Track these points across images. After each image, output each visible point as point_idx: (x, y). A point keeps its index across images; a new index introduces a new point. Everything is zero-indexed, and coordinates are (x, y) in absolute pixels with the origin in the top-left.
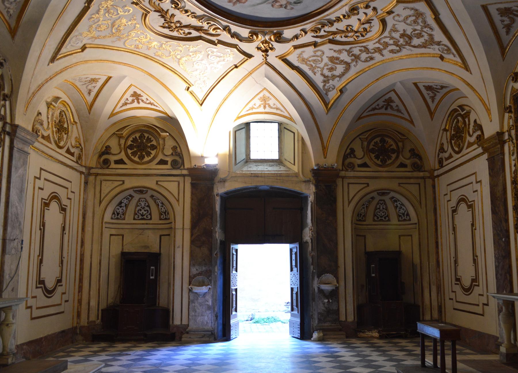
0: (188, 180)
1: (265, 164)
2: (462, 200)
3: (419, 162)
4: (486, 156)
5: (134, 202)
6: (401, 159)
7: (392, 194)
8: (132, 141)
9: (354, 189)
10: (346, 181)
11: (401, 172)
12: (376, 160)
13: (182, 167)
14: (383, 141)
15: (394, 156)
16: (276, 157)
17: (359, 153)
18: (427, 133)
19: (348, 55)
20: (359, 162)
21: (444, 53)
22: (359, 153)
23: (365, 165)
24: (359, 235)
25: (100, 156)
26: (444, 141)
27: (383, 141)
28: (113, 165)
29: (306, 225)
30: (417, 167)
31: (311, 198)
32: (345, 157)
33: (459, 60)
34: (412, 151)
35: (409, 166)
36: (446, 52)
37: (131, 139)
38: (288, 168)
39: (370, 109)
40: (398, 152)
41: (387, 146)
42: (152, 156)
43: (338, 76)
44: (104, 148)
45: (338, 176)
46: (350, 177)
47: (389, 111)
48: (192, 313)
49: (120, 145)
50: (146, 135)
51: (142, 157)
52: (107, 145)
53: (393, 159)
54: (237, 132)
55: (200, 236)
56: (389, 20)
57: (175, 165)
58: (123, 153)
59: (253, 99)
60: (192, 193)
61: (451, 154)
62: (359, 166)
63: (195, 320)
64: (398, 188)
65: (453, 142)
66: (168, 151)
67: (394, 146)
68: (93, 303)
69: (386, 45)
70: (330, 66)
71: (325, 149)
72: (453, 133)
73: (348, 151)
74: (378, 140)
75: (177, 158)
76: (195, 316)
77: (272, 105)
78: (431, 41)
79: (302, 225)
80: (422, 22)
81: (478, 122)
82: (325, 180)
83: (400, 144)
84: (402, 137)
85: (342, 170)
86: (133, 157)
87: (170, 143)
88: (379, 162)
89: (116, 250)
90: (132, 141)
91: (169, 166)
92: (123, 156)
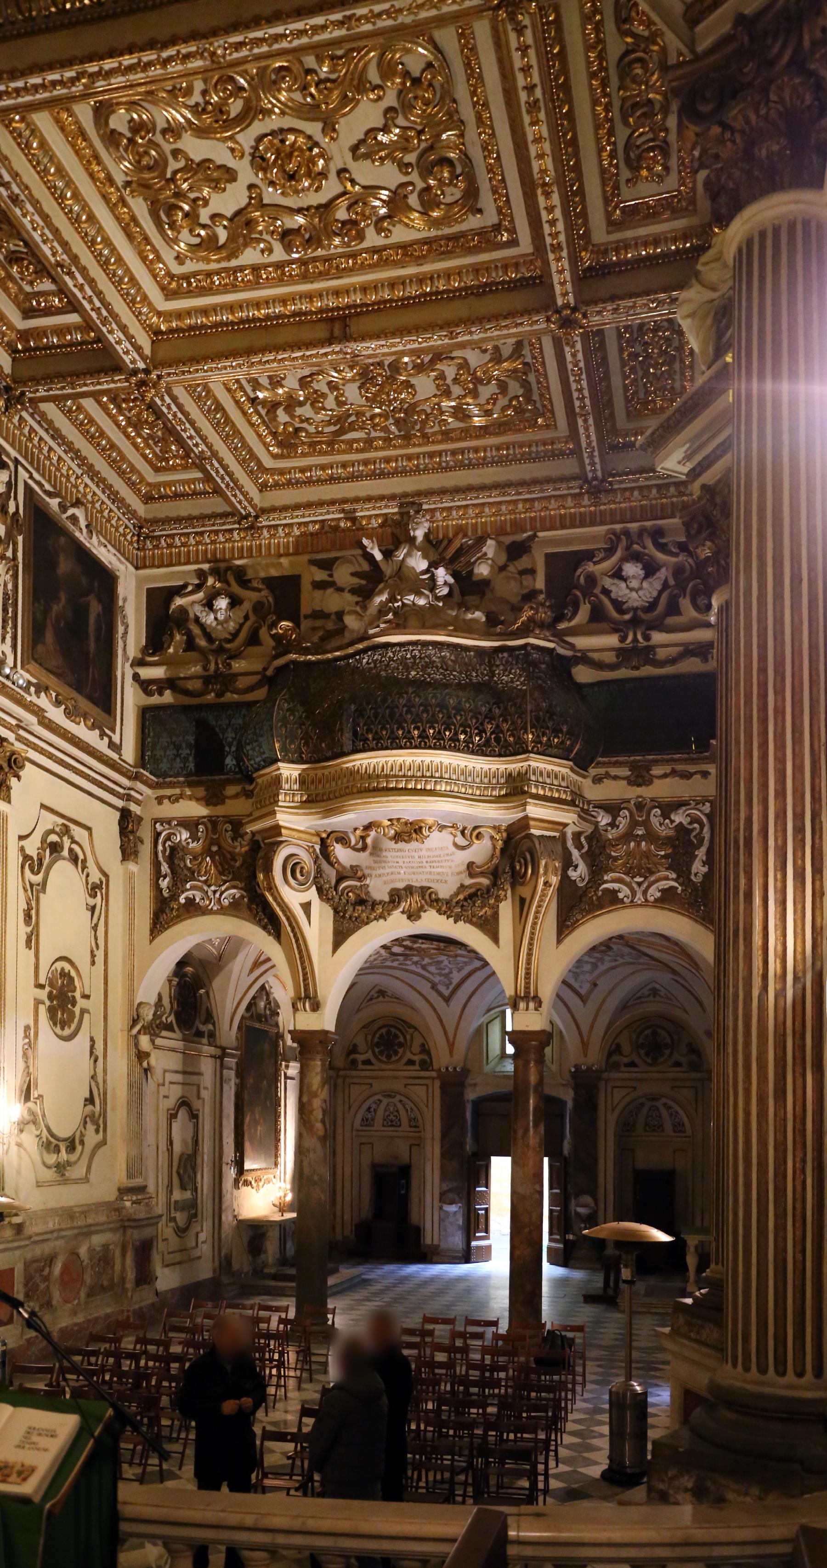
0: (437, 1083)
5: (383, 1106)
9: (618, 1094)
23: (632, 1064)
24: (624, 1150)
32: (610, 1055)
34: (690, 1045)
51: (389, 1057)
55: (451, 1148)
62: (627, 1065)
66: (416, 1048)
67: (668, 1040)
75: (425, 1057)
83: (676, 1037)
87: (418, 1041)
88: (649, 1061)
89: (366, 1160)
91: (417, 1067)
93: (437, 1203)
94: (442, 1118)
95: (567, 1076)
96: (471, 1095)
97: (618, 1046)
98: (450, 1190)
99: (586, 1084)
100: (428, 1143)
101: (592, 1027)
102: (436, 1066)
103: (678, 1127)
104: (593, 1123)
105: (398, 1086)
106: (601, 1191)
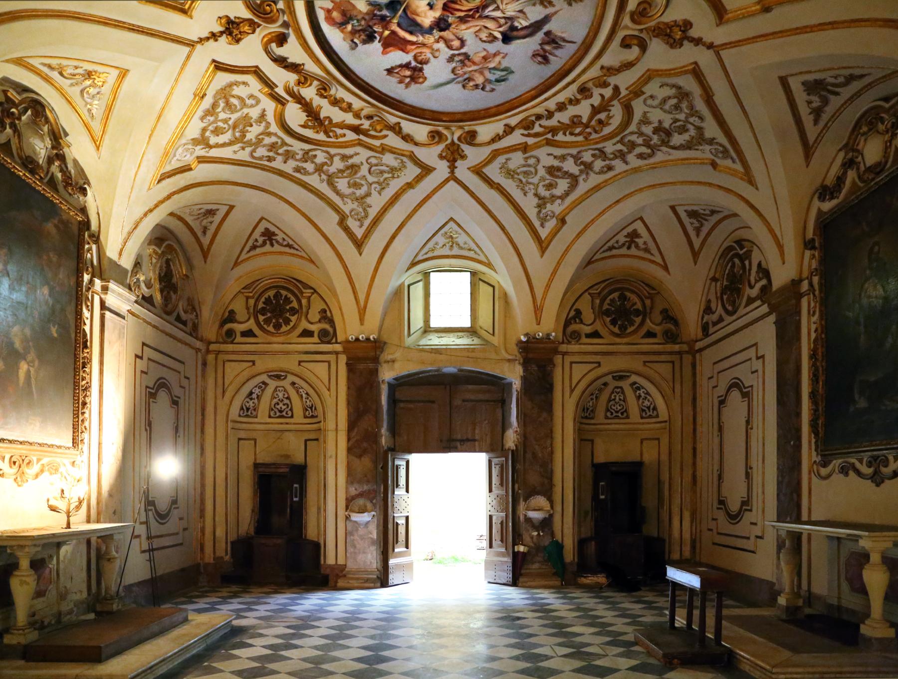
0: (343, 359)
1: (452, 335)
2: (736, 385)
3: (673, 327)
4: (772, 318)
6: (649, 325)
7: (634, 378)
8: (264, 303)
10: (568, 359)
11: (648, 345)
12: (612, 327)
13: (334, 340)
14: (623, 298)
15: (638, 320)
16: (467, 323)
18: (686, 286)
19: (575, 163)
20: (588, 330)
21: (719, 157)
23: (595, 335)
25: (222, 325)
26: (713, 297)
27: (623, 298)
28: (239, 339)
30: (671, 337)
32: (567, 323)
33: (738, 167)
35: (659, 335)
36: (720, 155)
37: (263, 299)
38: (484, 339)
39: (606, 247)
40: (644, 314)
41: (628, 307)
42: (292, 324)
43: (559, 197)
44: (227, 314)
45: (556, 351)
46: (573, 353)
47: (633, 251)
48: (350, 549)
49: (248, 308)
50: (284, 293)
51: (277, 326)
52: (229, 309)
53: (636, 325)
54: (411, 287)
56: (638, 106)
57: (327, 336)
58: (252, 321)
59: (434, 235)
61: (721, 316)
62: (588, 336)
63: (355, 559)
64: (640, 367)
65: (725, 297)
66: (314, 315)
67: (639, 306)
68: (220, 532)
69: (632, 146)
70: (547, 182)
71: (538, 310)
72: (725, 283)
73: (572, 313)
74: (616, 295)
75: (327, 326)
76: (355, 553)
77: (462, 245)
78: (700, 139)
80: (687, 107)
82: (537, 357)
83: (648, 302)
85: (563, 343)
86: (265, 326)
88: (616, 330)
90: (264, 303)
91: (316, 339)
92: (251, 324)
93: (342, 512)
94: (348, 403)
95: (515, 350)
97: (578, 312)
101: (548, 287)
102: (341, 337)
105: (289, 363)
106: (558, 490)
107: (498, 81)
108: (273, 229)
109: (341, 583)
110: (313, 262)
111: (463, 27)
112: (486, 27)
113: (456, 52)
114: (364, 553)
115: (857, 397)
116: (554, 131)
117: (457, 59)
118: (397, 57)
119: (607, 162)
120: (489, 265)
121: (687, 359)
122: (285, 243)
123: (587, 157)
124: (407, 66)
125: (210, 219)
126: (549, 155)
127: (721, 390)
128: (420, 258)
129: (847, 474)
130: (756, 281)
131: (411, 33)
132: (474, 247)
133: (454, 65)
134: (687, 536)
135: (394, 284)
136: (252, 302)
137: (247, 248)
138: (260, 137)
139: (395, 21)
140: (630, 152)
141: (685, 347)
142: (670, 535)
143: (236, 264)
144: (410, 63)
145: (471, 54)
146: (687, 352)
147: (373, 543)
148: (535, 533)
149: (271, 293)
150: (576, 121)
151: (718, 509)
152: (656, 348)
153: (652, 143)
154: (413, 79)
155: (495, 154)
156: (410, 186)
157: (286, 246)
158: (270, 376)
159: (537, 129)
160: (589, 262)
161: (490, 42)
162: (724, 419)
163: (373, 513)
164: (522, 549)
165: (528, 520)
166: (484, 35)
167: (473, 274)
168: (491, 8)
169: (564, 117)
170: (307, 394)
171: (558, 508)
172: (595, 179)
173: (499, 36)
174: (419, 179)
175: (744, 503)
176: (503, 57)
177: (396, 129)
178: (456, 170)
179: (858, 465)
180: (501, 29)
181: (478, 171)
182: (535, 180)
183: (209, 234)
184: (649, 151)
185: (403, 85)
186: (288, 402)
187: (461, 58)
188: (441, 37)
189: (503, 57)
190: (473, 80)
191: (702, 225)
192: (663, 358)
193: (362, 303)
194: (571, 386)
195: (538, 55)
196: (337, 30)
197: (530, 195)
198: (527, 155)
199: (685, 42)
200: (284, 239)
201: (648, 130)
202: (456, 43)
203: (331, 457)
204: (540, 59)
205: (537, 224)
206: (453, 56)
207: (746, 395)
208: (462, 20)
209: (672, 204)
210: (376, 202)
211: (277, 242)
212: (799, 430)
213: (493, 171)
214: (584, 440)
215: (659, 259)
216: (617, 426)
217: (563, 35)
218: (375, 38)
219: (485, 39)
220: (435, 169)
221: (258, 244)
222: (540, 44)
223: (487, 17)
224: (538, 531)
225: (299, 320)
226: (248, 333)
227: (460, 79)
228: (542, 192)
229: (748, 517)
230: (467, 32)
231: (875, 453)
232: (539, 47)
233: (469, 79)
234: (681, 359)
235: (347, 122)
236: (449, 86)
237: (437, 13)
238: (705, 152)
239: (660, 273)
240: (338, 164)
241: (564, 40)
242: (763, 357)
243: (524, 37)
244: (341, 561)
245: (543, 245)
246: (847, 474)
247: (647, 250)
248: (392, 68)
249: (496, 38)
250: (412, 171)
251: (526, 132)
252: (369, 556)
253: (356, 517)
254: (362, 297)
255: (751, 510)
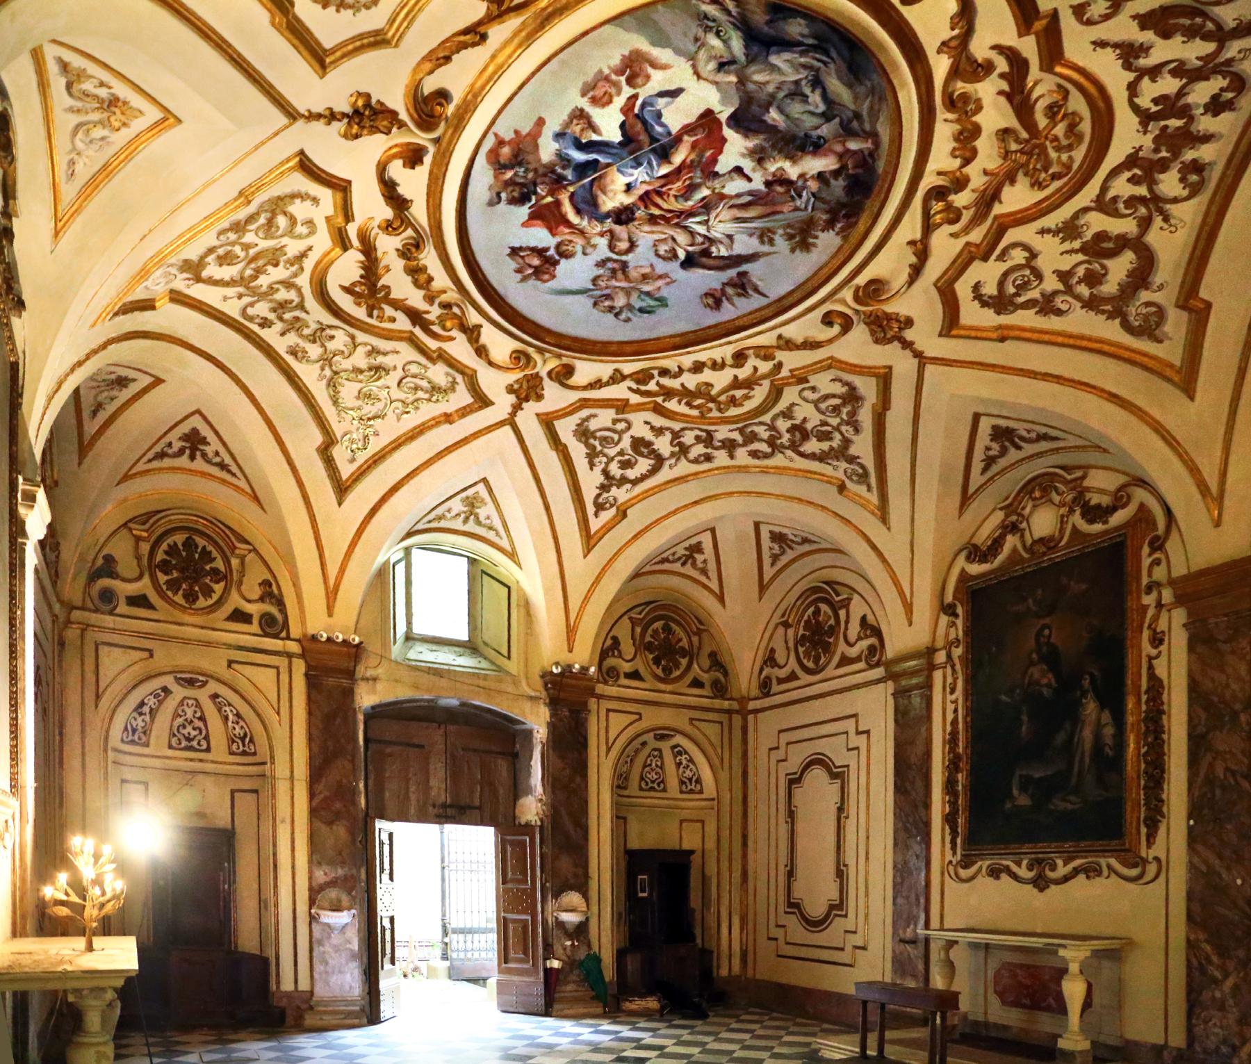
0: (300, 667)
1: (446, 649)
3: (722, 679)
8: (166, 553)
9: (617, 722)
11: (694, 697)
12: (654, 667)
13: (284, 634)
14: (667, 629)
15: (684, 662)
16: (464, 636)
17: (628, 648)
18: (743, 625)
20: (627, 667)
21: (852, 480)
22: (628, 648)
23: (635, 675)
27: (667, 629)
29: (529, 791)
30: (720, 690)
31: (541, 733)
32: (604, 655)
33: (874, 498)
34: (713, 655)
35: (707, 685)
36: (855, 478)
37: (164, 546)
40: (691, 654)
41: (674, 642)
42: (215, 597)
49: (138, 558)
50: (201, 542)
51: (191, 597)
52: (105, 552)
53: (682, 668)
56: (790, 395)
58: (146, 580)
60: (310, 700)
61: (793, 672)
62: (628, 676)
65: (801, 650)
67: (685, 643)
71: (571, 631)
73: (609, 642)
74: (659, 625)
75: (274, 610)
78: (842, 453)
79: (518, 789)
80: (848, 413)
81: (870, 618)
83: (695, 639)
84: (700, 626)
85: (598, 682)
86: (169, 593)
88: (659, 672)
90: (166, 553)
91: (255, 627)
93: (302, 908)
94: (310, 739)
95: (539, 683)
96: (366, 698)
97: (616, 641)
98: (332, 884)
99: (568, 694)
100: (282, 788)
101: (587, 599)
102: (295, 631)
103: (691, 784)
104: (581, 768)
105: (214, 662)
107: (641, 310)
108: (205, 431)
109: (309, 1020)
110: (256, 498)
111: (647, 228)
112: (674, 239)
113: (615, 257)
114: (340, 972)
115: (1015, 792)
116: (668, 393)
117: (610, 265)
118: (540, 237)
119: (709, 451)
120: (512, 555)
121: (737, 720)
122: (217, 460)
123: (688, 438)
124: (540, 252)
125: (115, 393)
126: (647, 423)
127: (794, 764)
128: (420, 526)
129: (998, 878)
130: (859, 638)
131: (578, 212)
132: (497, 524)
133: (601, 271)
134: (736, 947)
135: (381, 559)
136: (145, 548)
137: (150, 455)
138: (276, 286)
139: (571, 189)
140: (745, 444)
141: (735, 705)
142: (719, 946)
143: (126, 477)
144: (547, 249)
145: (631, 265)
146: (737, 712)
147: (353, 956)
148: (569, 943)
149: (179, 538)
150: (703, 391)
151: (786, 913)
152: (705, 702)
153: (779, 442)
154: (538, 273)
155: (584, 403)
156: (448, 418)
157: (216, 464)
158: (178, 680)
159: (652, 386)
160: (637, 575)
161: (664, 258)
162: (795, 801)
163: (354, 911)
164: (556, 964)
165: (560, 924)
166: (663, 249)
167: (472, 562)
168: (698, 219)
169: (691, 381)
170: (238, 715)
171: (595, 908)
172: (684, 467)
173: (682, 255)
174: (464, 412)
175: (832, 907)
176: (668, 284)
177: (472, 333)
178: (520, 413)
179: (1014, 868)
180: (690, 249)
181: (548, 422)
182: (612, 452)
183: (103, 416)
184: (769, 450)
185: (519, 276)
186: (200, 724)
187: (616, 265)
188: (611, 231)
189: (668, 284)
190: (612, 299)
191: (783, 553)
192: (711, 716)
193: (332, 582)
194: (607, 743)
195: (712, 295)
196: (492, 172)
197: (598, 469)
198: (620, 416)
199: (896, 343)
200: (217, 454)
201: (783, 425)
202: (624, 245)
203: (283, 821)
204: (710, 301)
205: (590, 509)
206: (609, 259)
207: (838, 775)
208: (653, 220)
209: (757, 519)
210: (389, 429)
211: (204, 455)
212: (927, 824)
213: (566, 429)
214: (620, 819)
215: (714, 585)
216: (656, 801)
217: (759, 283)
218: (530, 200)
219: (662, 253)
220: (493, 404)
221: (170, 451)
222: (724, 284)
223: (685, 228)
224: (572, 940)
225: (226, 591)
226: (139, 601)
227: (598, 293)
228: (615, 469)
229: (838, 925)
230: (646, 237)
231: (1040, 856)
232: (719, 287)
233: (608, 297)
234: (730, 720)
235: (410, 303)
236: (579, 297)
237: (628, 200)
238: (839, 469)
239: (709, 602)
240: (360, 359)
241: (757, 290)
242: (868, 732)
243: (710, 268)
244: (304, 985)
245: (590, 540)
246: (998, 878)
247: (704, 572)
248: (521, 249)
249: (675, 256)
250: (462, 397)
251: (635, 386)
252: (348, 977)
253: (329, 918)
254: (333, 572)
255: (846, 916)
